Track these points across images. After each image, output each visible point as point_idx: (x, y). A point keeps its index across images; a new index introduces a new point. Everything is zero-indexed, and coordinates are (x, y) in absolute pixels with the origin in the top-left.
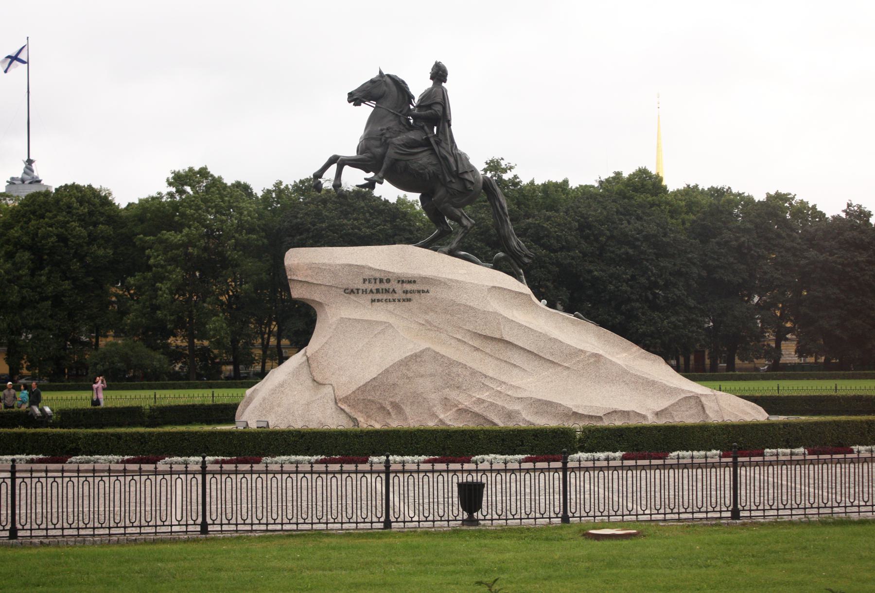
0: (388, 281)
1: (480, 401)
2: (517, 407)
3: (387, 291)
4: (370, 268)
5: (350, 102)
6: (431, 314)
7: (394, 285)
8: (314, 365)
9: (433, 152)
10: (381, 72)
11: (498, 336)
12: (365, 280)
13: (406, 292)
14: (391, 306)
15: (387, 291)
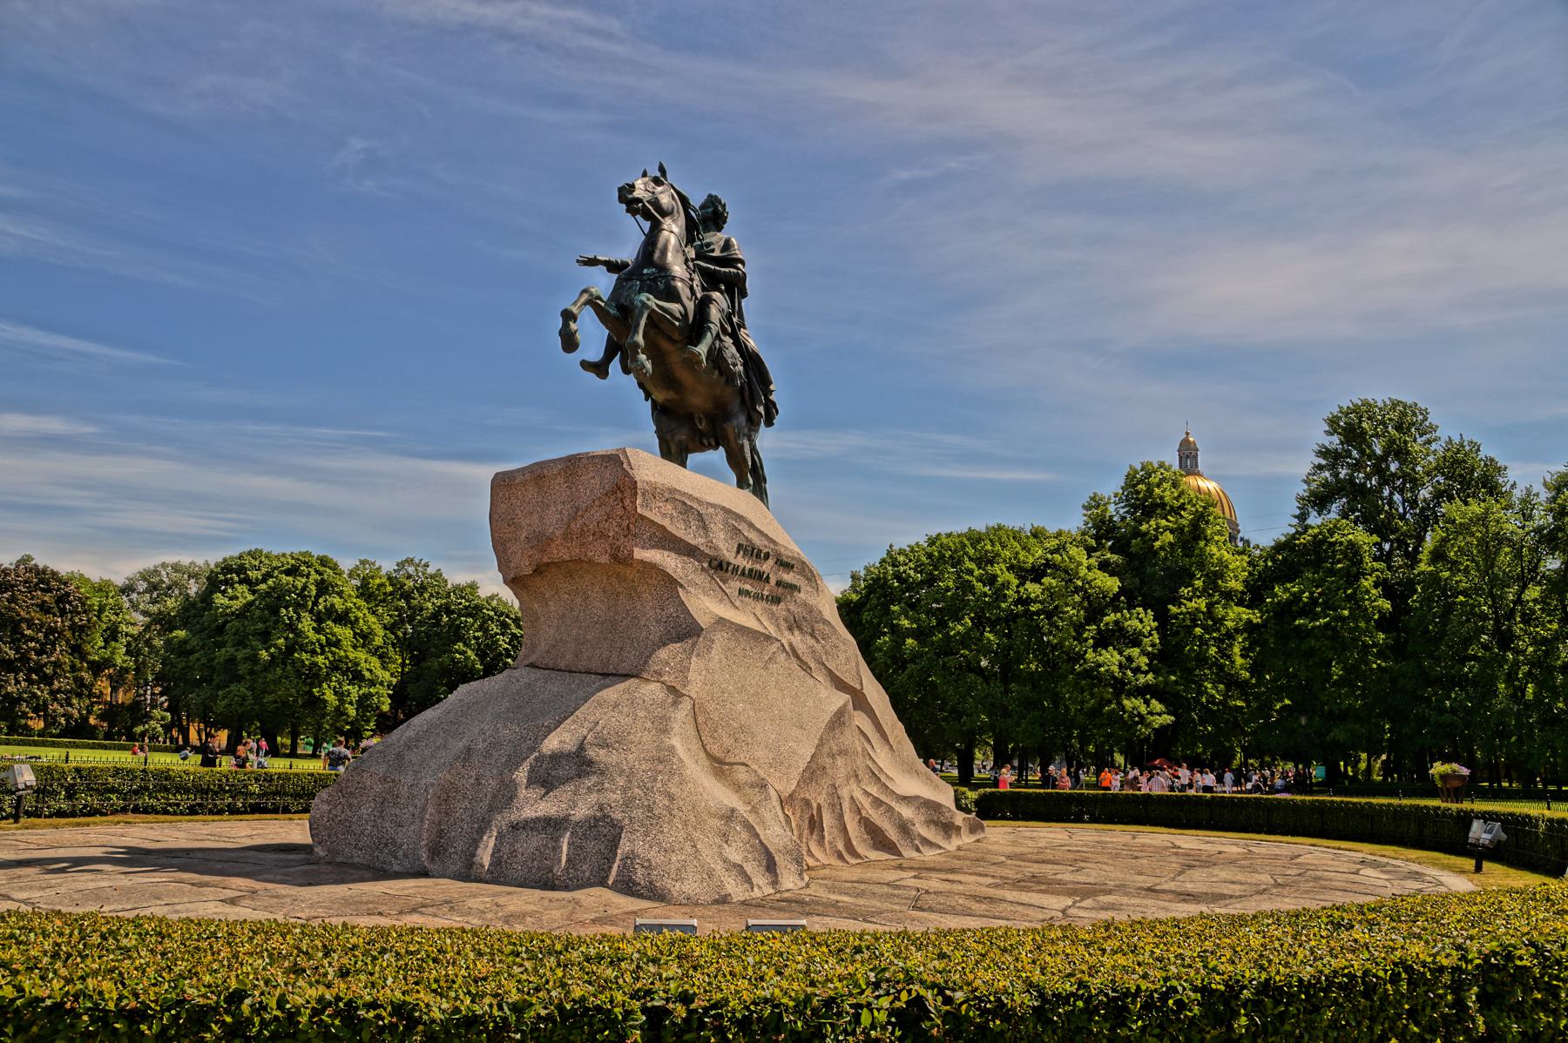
0: (767, 556)
1: (877, 803)
2: (907, 812)
3: (759, 577)
4: (751, 525)
5: (622, 199)
6: (797, 632)
7: (767, 567)
8: (700, 720)
9: (738, 343)
10: (662, 169)
11: (858, 687)
12: (740, 546)
13: (779, 583)
14: (759, 607)
15: (759, 577)
